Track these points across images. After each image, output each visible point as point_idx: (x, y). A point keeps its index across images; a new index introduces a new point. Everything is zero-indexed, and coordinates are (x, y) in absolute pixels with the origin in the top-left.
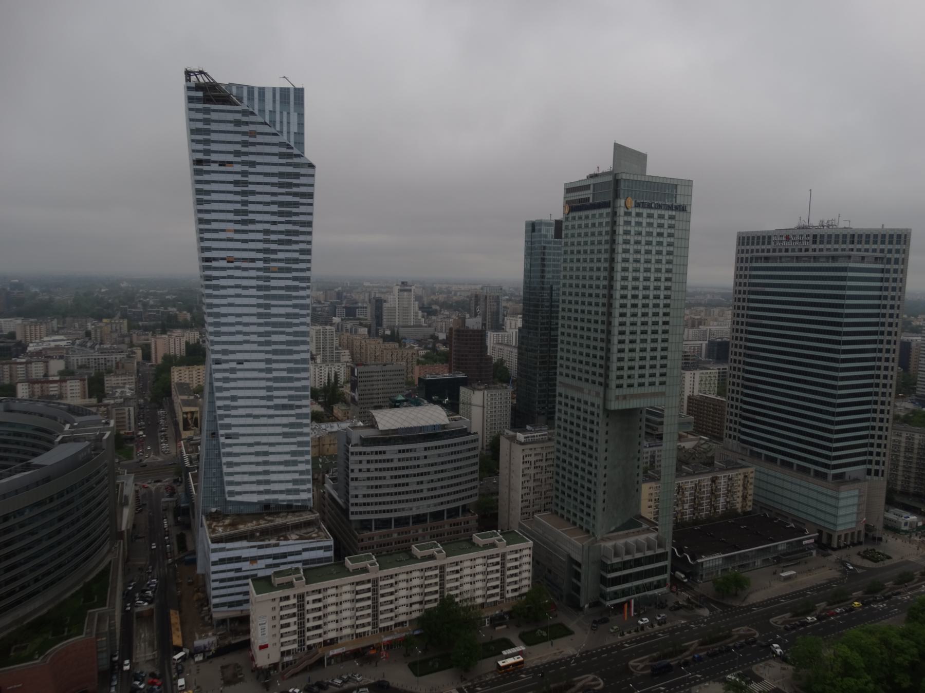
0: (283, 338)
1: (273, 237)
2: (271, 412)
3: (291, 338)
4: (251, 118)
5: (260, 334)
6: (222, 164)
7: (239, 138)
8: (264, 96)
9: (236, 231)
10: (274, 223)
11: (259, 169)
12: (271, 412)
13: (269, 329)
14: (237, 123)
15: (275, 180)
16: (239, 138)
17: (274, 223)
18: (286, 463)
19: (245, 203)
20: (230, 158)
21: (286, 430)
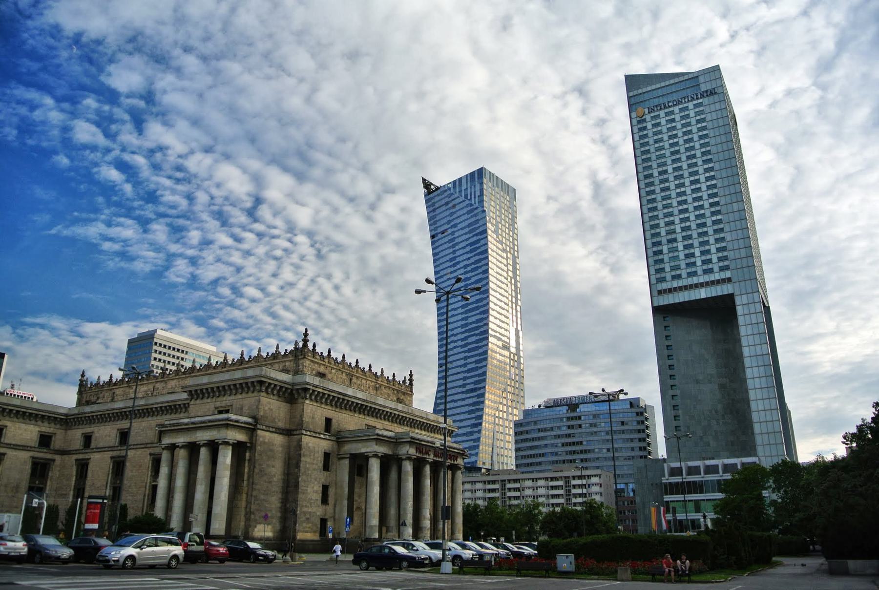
0: (474, 339)
1: (469, 268)
2: (464, 396)
3: (478, 337)
4: (453, 197)
5: (462, 340)
6: (443, 233)
7: (448, 213)
8: (461, 182)
9: (451, 273)
10: (469, 259)
11: (459, 226)
12: (464, 396)
13: (467, 334)
14: (447, 204)
15: (467, 230)
16: (448, 213)
17: (469, 259)
18: (467, 434)
19: (454, 252)
20: (446, 227)
21: (471, 408)
